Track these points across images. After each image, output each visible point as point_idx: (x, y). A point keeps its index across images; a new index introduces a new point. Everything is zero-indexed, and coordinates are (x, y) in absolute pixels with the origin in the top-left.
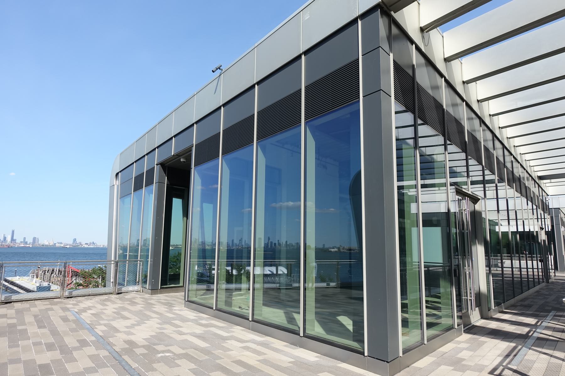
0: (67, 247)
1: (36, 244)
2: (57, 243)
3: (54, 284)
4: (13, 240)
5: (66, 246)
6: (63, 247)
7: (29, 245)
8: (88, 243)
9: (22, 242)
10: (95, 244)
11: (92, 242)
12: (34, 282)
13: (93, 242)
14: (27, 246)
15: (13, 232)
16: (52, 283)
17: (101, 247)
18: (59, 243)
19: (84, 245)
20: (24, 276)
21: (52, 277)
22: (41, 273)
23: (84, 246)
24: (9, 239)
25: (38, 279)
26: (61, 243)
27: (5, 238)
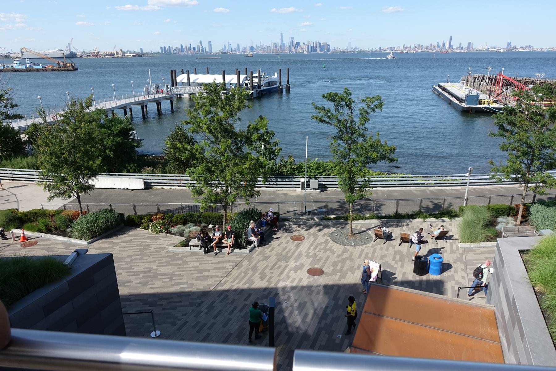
0: (500, 52)
1: (471, 50)
2: (491, 47)
3: (484, 93)
4: (450, 46)
5: (500, 51)
6: (496, 52)
7: (464, 50)
8: (524, 46)
9: (458, 48)
10: (532, 48)
11: (528, 46)
12: (464, 89)
13: (530, 45)
14: (463, 51)
15: (451, 37)
16: (481, 91)
17: (539, 50)
18: (492, 48)
19: (518, 49)
20: (455, 82)
21: (482, 84)
22: (471, 80)
23: (519, 50)
24: (447, 45)
25: (468, 86)
26: (495, 48)
27: (444, 44)
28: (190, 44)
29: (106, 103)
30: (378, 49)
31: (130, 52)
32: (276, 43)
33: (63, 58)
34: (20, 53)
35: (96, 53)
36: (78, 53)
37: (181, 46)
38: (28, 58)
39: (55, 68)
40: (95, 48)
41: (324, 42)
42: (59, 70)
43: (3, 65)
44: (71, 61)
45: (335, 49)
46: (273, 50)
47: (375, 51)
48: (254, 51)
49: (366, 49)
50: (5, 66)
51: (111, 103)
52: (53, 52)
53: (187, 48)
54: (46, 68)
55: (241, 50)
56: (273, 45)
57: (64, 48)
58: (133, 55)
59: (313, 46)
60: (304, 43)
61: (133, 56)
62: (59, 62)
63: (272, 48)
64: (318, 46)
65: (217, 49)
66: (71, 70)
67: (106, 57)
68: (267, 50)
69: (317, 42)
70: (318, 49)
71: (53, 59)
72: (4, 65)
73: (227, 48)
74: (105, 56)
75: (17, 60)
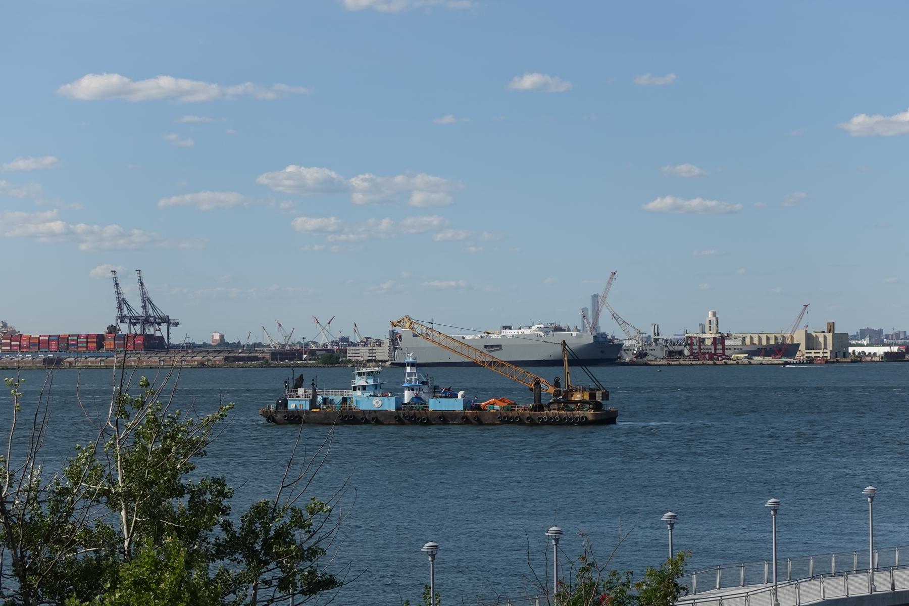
29: (726, 592)
31: (877, 338)
33: (557, 363)
34: (387, 341)
35: (708, 342)
36: (627, 343)
38: (412, 365)
39: (519, 410)
40: (710, 314)
42: (533, 423)
43: (310, 391)
44: (594, 379)
50: (319, 399)
51: (747, 597)
52: (523, 337)
54: (478, 408)
57: (570, 317)
58: (887, 349)
61: (886, 353)
62: (537, 383)
66: (584, 422)
67: (757, 359)
71: (520, 369)
72: (315, 396)
74: (752, 353)
75: (369, 374)
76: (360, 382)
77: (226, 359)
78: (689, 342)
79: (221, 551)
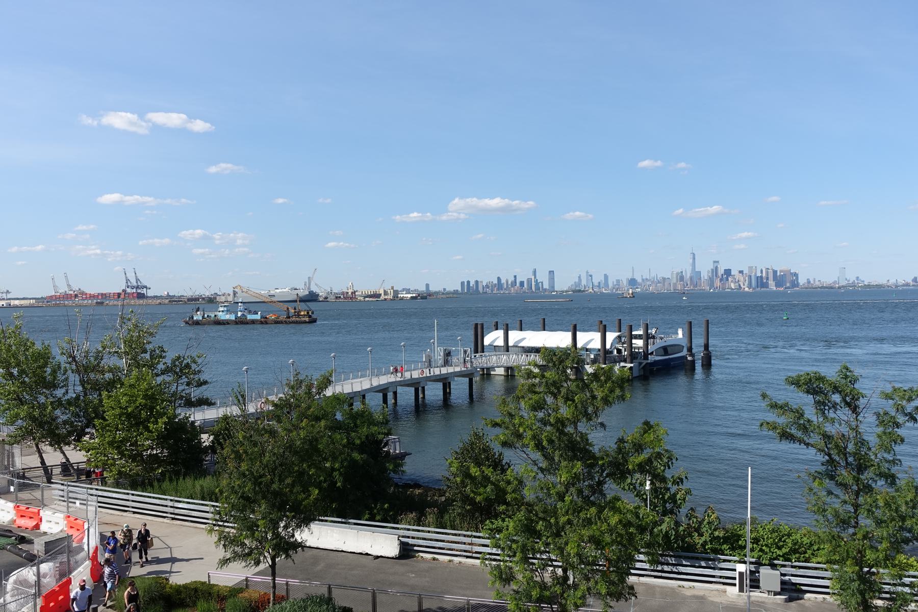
28: (515, 277)
30: (910, 281)
31: (408, 291)
32: (682, 272)
33: (295, 301)
34: (232, 294)
35: (350, 293)
36: (320, 294)
37: (499, 279)
38: (241, 303)
39: (281, 318)
41: (782, 269)
42: (286, 322)
43: (202, 313)
44: (308, 307)
45: (809, 282)
46: (675, 284)
47: (904, 285)
48: (637, 288)
49: (882, 280)
50: (206, 316)
51: (361, 382)
52: (283, 292)
53: (510, 283)
54: (266, 318)
55: (611, 285)
56: (675, 276)
57: (300, 286)
58: (412, 295)
59: (761, 277)
60: (741, 272)
62: (288, 309)
63: (674, 281)
64: (771, 276)
65: (563, 284)
66: (305, 322)
67: (367, 299)
68: (664, 285)
69: (768, 269)
70: (772, 283)
71: (279, 303)
72: (204, 314)
73: (584, 282)
74: (365, 297)
75: (225, 306)
76: (221, 309)
77: (170, 301)
78: (343, 293)
79: (163, 372)
